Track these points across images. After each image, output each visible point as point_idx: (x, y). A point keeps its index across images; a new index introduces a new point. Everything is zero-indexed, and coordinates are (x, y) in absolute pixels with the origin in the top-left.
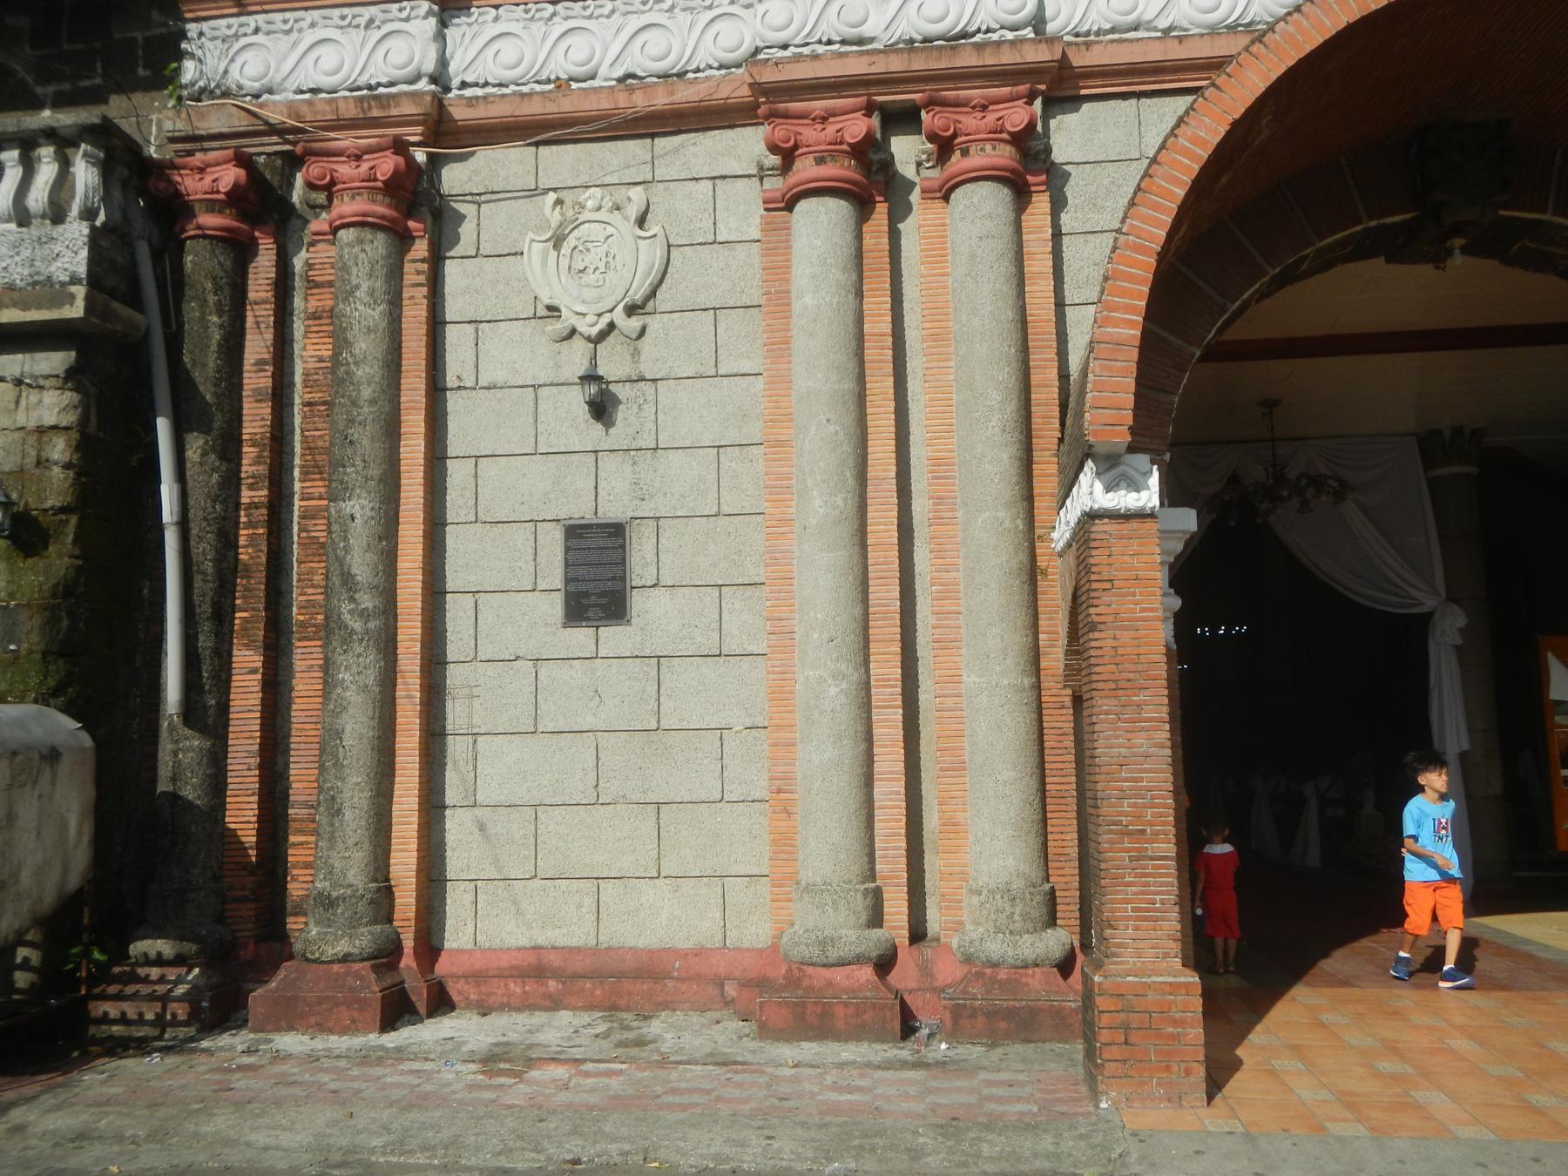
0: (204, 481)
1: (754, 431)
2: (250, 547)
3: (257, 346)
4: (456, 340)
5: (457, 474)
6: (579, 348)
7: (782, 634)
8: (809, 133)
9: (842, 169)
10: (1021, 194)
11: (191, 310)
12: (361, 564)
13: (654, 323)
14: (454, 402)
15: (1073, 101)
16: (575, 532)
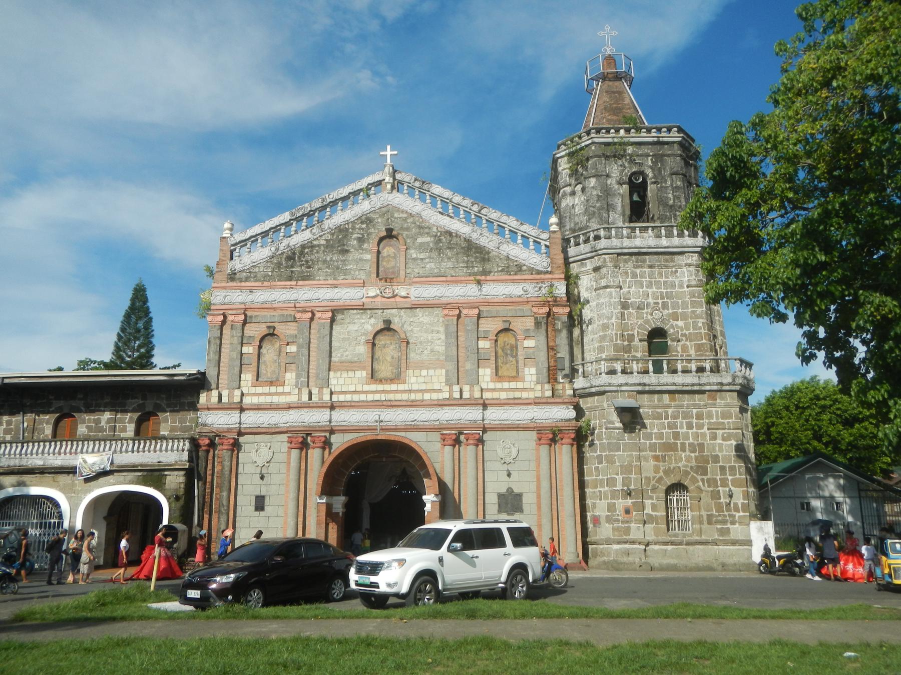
0: (201, 489)
1: (285, 482)
2: (207, 499)
3: (210, 467)
4: (240, 466)
5: (239, 487)
6: (259, 468)
7: (286, 514)
8: (294, 440)
9: (299, 445)
10: (324, 448)
11: (200, 462)
12: (225, 503)
13: (271, 465)
14: (239, 476)
15: (334, 433)
16: (257, 497)
